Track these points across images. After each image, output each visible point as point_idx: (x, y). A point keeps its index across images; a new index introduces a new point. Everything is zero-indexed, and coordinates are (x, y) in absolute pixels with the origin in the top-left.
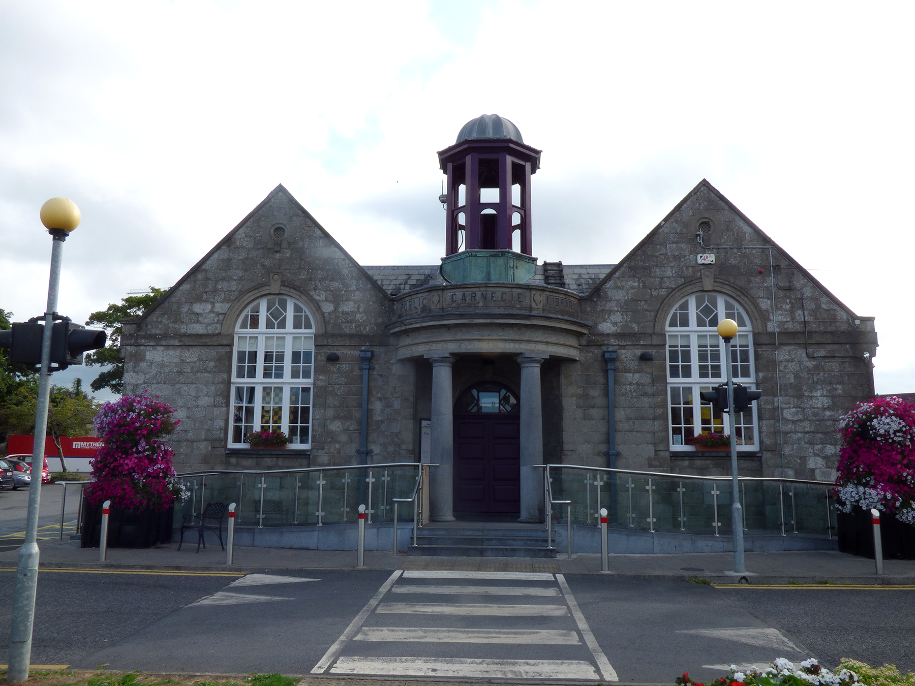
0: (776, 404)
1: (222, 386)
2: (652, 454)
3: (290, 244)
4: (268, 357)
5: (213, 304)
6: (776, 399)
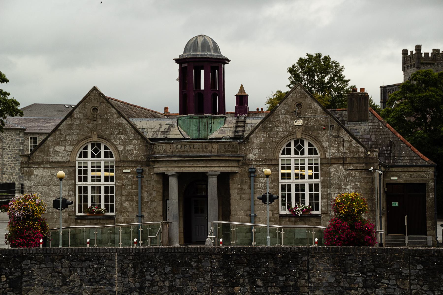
0: (329, 192)
1: (72, 186)
3: (101, 116)
5: (65, 147)
6: (329, 190)
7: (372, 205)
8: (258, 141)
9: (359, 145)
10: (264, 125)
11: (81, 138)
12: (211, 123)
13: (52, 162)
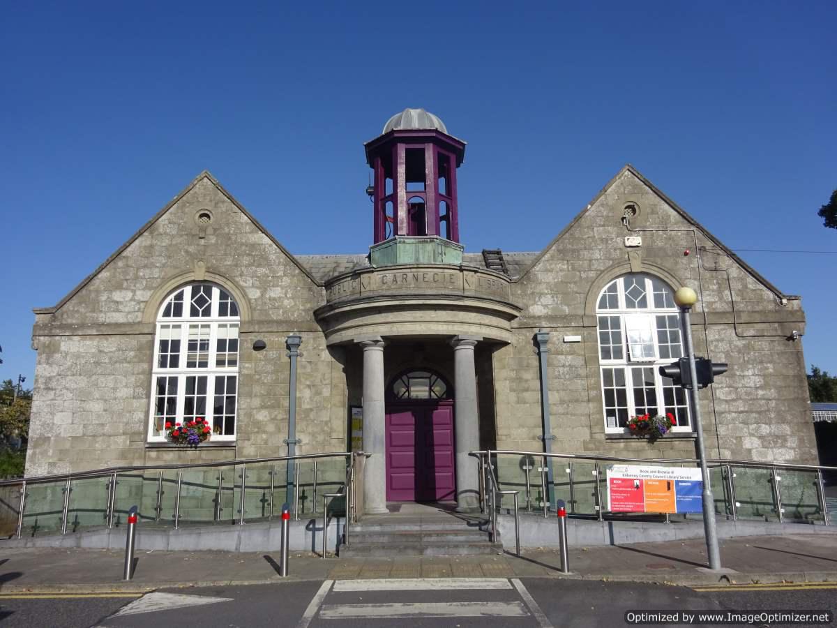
1: (142, 376)
2: (588, 437)
3: (215, 230)
4: (192, 346)
5: (134, 292)
7: (805, 411)
8: (550, 278)
9: (762, 287)
10: (561, 247)
11: (170, 275)
12: (441, 254)
13: (103, 324)
